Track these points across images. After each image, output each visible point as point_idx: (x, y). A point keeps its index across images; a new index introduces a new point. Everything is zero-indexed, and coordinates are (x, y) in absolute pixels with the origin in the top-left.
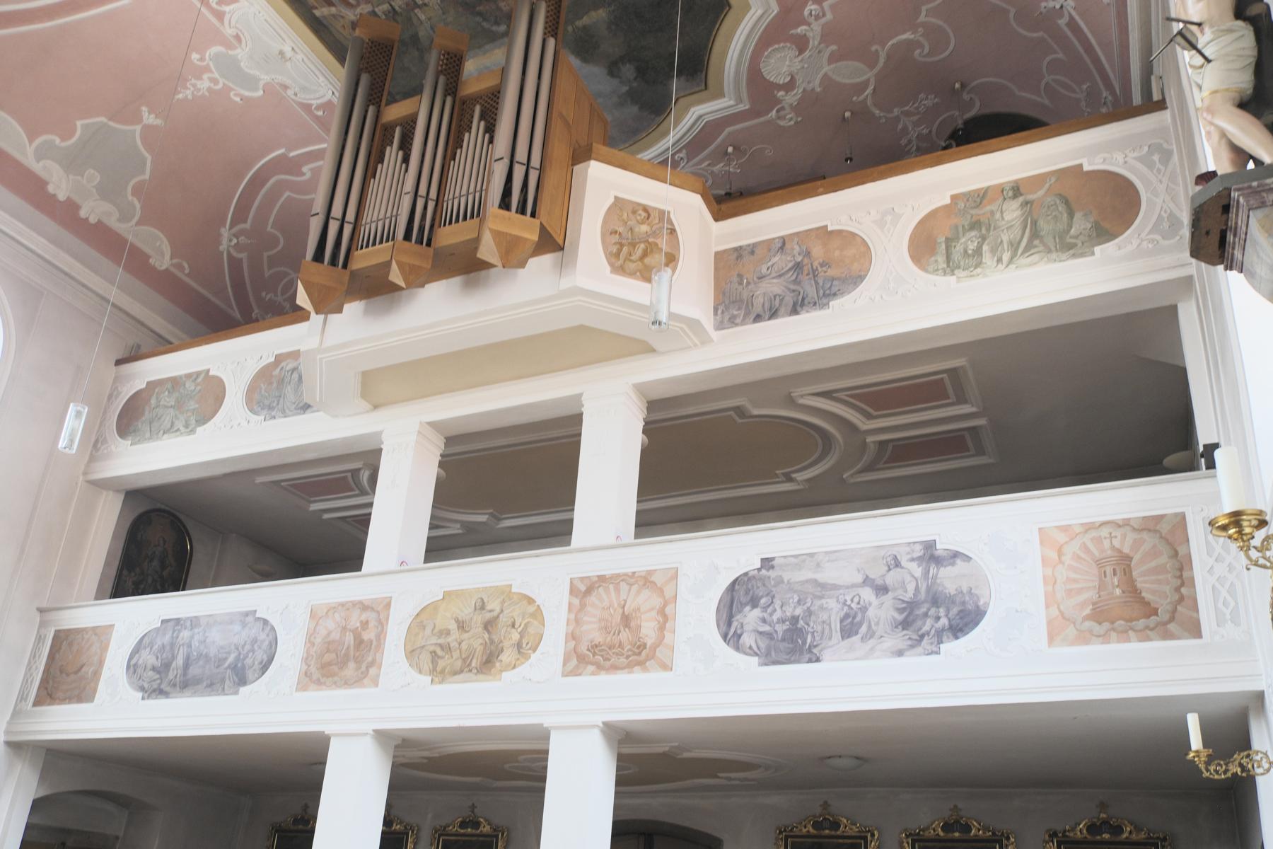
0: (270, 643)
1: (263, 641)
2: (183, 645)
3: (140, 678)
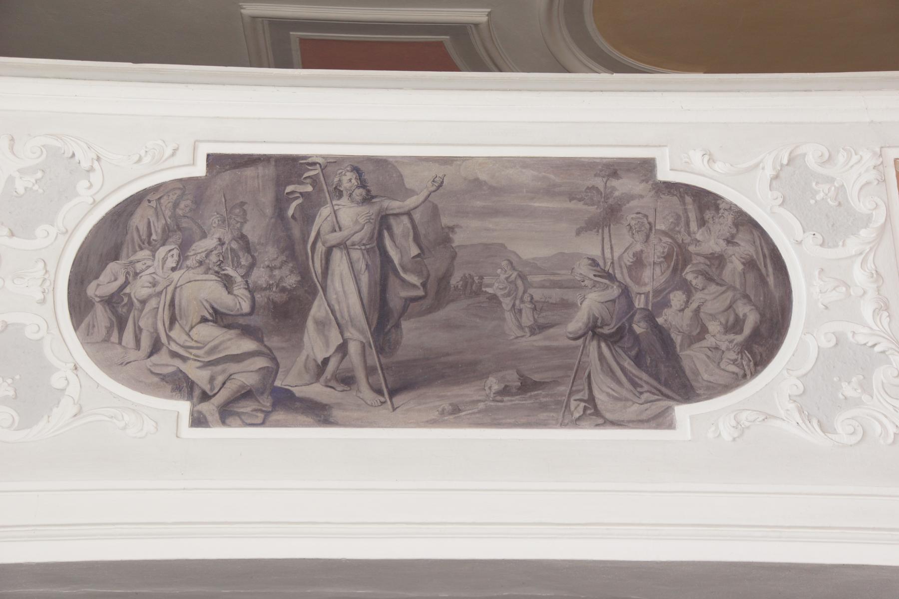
0: (750, 264)
1: (718, 260)
2: (343, 245)
3: (156, 347)
